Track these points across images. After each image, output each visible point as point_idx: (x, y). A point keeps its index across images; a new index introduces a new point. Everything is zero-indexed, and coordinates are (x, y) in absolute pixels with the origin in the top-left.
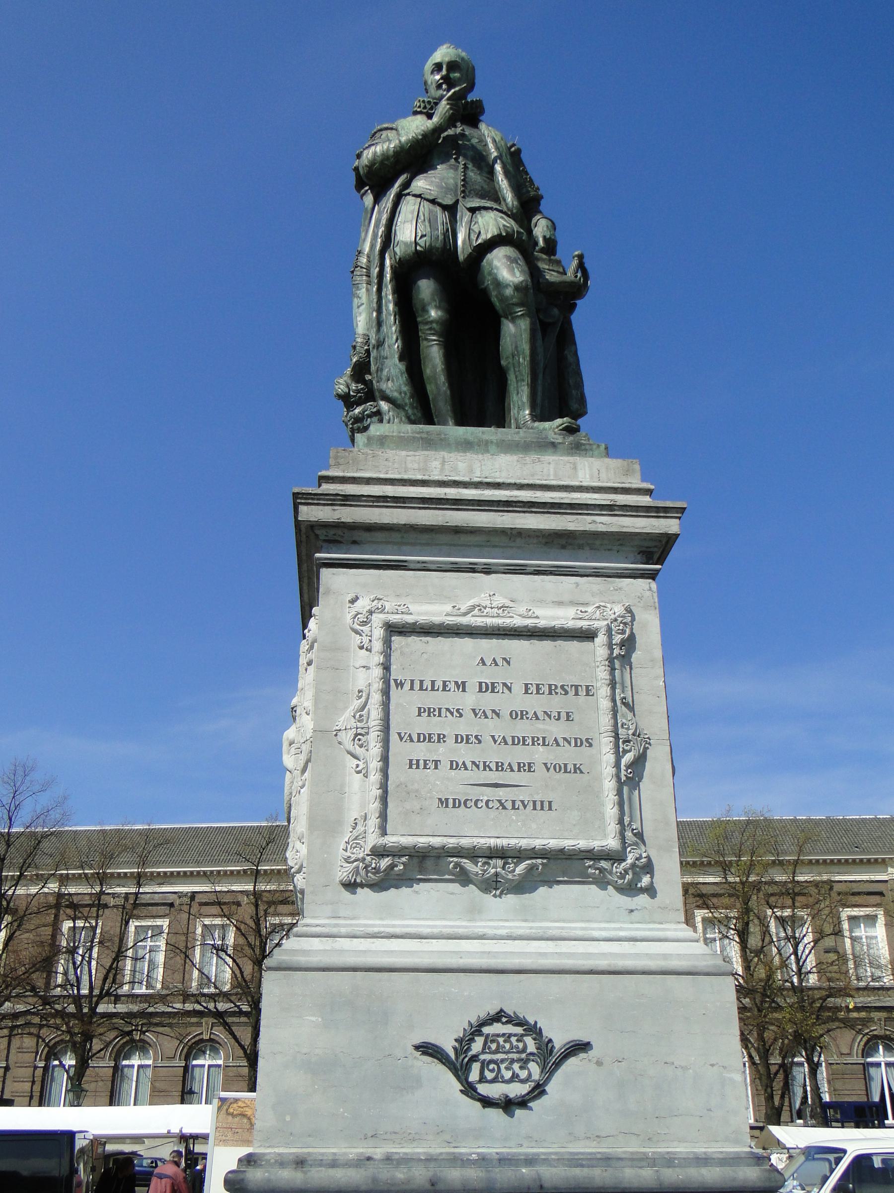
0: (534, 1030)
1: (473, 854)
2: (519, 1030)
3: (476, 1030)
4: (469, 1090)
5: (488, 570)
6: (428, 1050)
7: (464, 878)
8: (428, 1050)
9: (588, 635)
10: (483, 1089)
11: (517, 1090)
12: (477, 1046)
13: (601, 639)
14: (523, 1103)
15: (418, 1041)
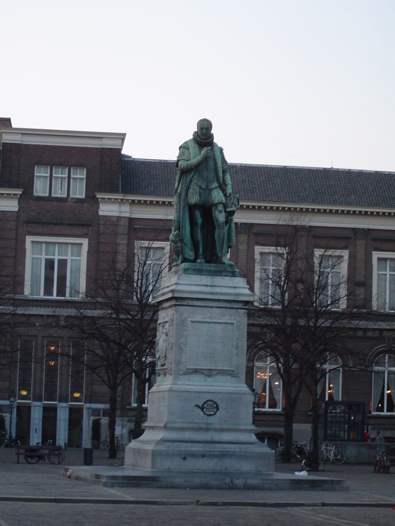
0: (216, 403)
1: (206, 370)
2: (213, 403)
3: (205, 403)
4: (204, 413)
5: (212, 307)
6: (197, 406)
7: (204, 374)
8: (197, 406)
9: (233, 324)
10: (207, 413)
11: (213, 413)
12: (205, 405)
13: (235, 325)
14: (213, 415)
15: (195, 404)
